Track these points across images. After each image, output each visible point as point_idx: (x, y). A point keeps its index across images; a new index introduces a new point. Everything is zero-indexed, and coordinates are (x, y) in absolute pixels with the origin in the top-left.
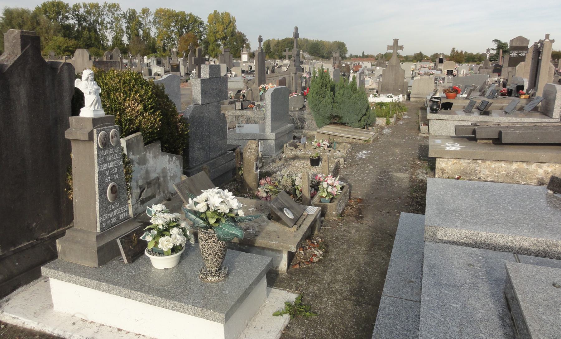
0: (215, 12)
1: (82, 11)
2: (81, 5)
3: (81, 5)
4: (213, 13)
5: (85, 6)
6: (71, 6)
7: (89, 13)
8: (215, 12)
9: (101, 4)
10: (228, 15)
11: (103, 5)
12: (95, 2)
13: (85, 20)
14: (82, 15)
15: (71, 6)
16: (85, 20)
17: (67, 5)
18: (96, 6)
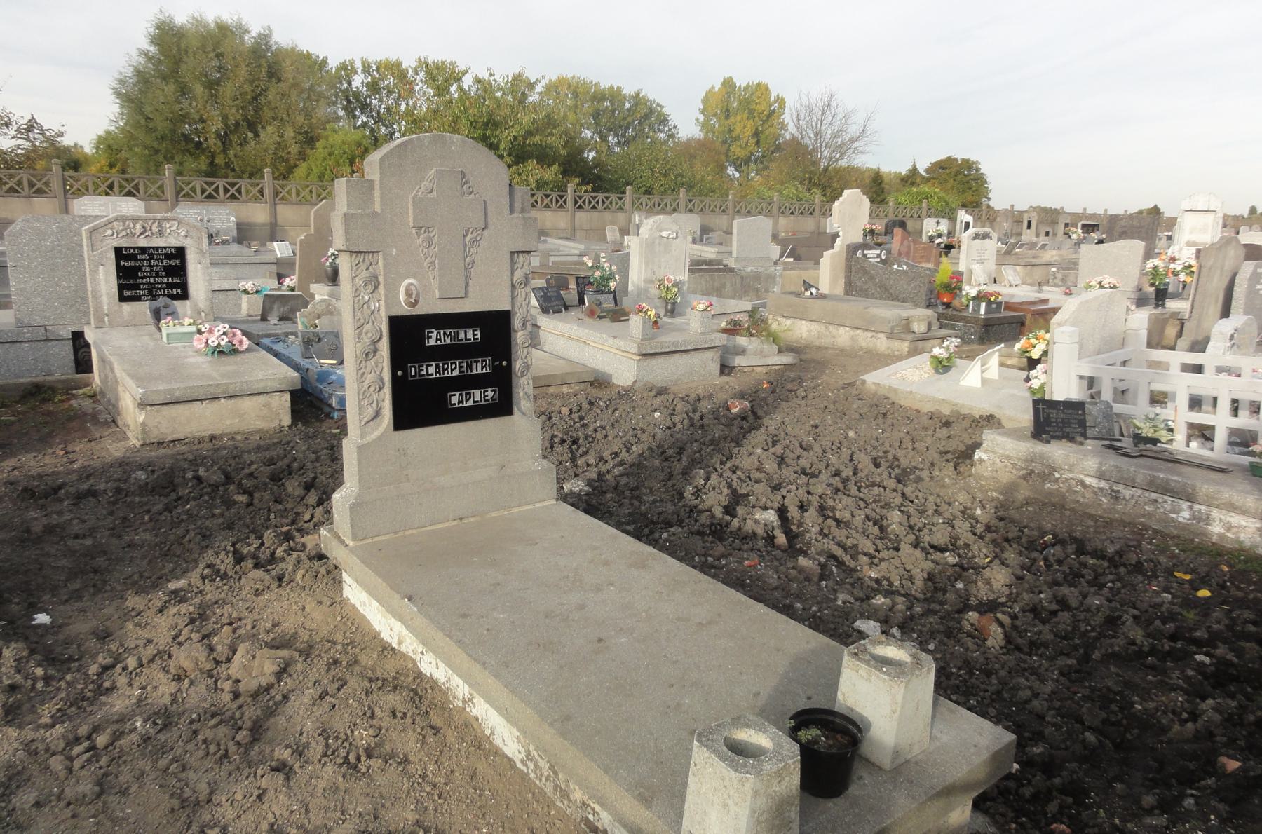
0: (728, 84)
1: (358, 81)
2: (359, 65)
3: (359, 65)
4: (718, 86)
5: (367, 68)
6: (333, 64)
7: (374, 87)
8: (728, 84)
9: (409, 63)
10: (762, 89)
11: (414, 65)
12: (393, 58)
13: (364, 107)
14: (357, 95)
15: (333, 64)
16: (364, 107)
17: (324, 62)
18: (395, 68)
